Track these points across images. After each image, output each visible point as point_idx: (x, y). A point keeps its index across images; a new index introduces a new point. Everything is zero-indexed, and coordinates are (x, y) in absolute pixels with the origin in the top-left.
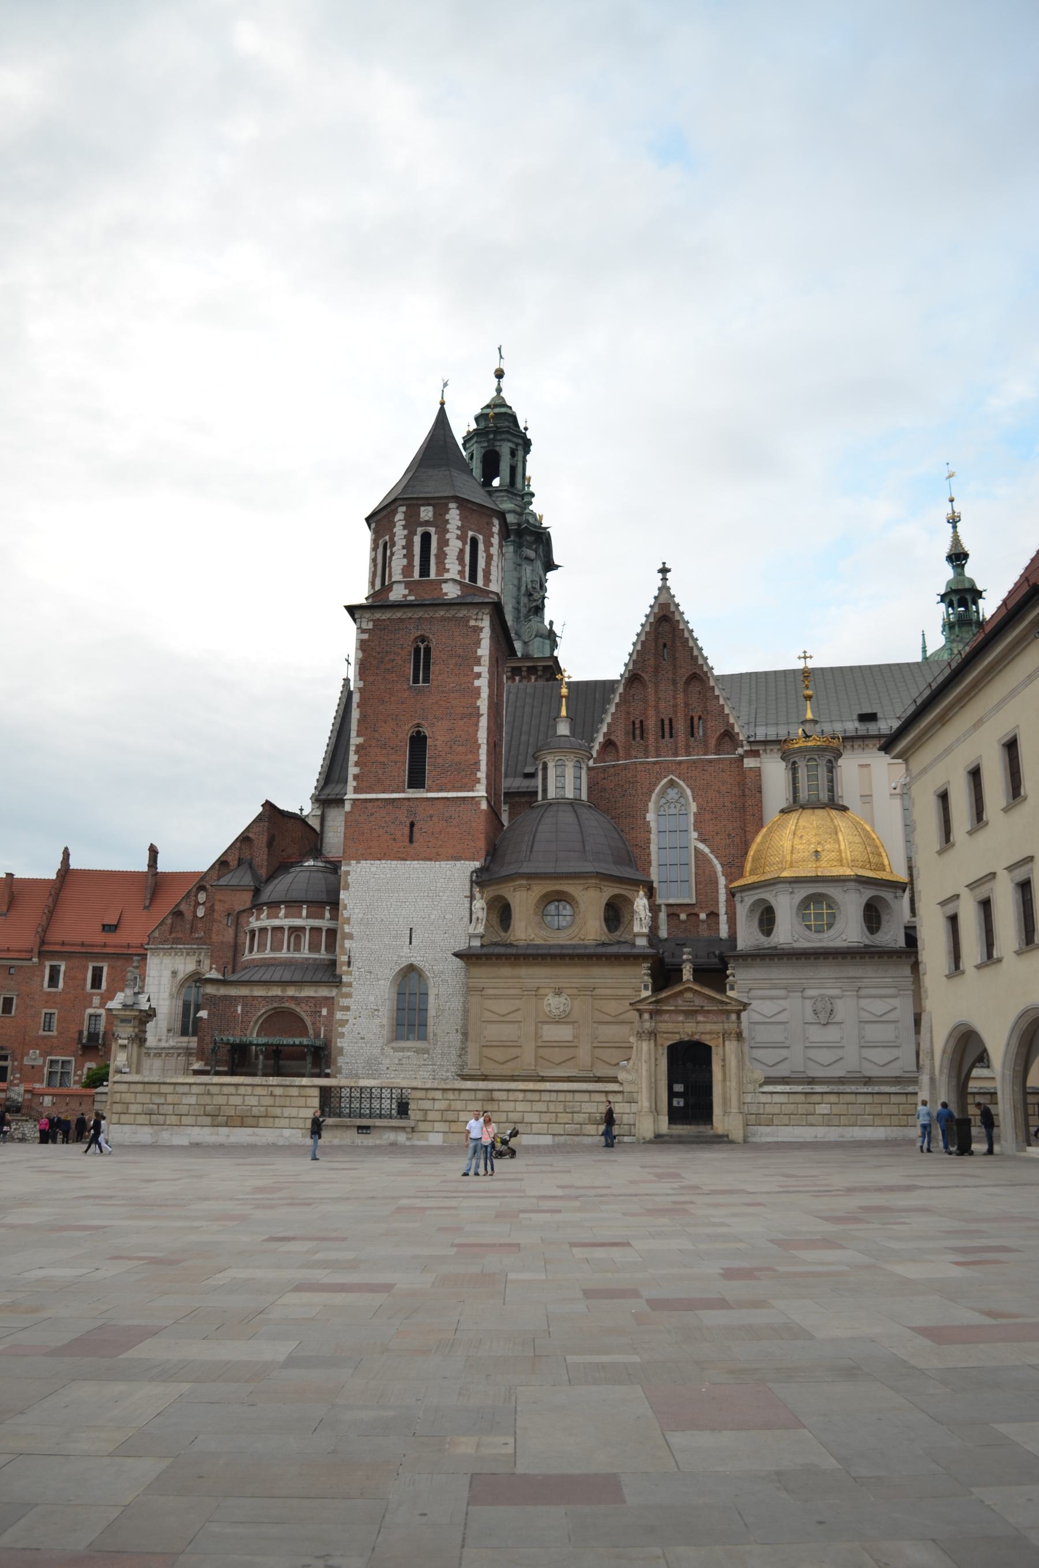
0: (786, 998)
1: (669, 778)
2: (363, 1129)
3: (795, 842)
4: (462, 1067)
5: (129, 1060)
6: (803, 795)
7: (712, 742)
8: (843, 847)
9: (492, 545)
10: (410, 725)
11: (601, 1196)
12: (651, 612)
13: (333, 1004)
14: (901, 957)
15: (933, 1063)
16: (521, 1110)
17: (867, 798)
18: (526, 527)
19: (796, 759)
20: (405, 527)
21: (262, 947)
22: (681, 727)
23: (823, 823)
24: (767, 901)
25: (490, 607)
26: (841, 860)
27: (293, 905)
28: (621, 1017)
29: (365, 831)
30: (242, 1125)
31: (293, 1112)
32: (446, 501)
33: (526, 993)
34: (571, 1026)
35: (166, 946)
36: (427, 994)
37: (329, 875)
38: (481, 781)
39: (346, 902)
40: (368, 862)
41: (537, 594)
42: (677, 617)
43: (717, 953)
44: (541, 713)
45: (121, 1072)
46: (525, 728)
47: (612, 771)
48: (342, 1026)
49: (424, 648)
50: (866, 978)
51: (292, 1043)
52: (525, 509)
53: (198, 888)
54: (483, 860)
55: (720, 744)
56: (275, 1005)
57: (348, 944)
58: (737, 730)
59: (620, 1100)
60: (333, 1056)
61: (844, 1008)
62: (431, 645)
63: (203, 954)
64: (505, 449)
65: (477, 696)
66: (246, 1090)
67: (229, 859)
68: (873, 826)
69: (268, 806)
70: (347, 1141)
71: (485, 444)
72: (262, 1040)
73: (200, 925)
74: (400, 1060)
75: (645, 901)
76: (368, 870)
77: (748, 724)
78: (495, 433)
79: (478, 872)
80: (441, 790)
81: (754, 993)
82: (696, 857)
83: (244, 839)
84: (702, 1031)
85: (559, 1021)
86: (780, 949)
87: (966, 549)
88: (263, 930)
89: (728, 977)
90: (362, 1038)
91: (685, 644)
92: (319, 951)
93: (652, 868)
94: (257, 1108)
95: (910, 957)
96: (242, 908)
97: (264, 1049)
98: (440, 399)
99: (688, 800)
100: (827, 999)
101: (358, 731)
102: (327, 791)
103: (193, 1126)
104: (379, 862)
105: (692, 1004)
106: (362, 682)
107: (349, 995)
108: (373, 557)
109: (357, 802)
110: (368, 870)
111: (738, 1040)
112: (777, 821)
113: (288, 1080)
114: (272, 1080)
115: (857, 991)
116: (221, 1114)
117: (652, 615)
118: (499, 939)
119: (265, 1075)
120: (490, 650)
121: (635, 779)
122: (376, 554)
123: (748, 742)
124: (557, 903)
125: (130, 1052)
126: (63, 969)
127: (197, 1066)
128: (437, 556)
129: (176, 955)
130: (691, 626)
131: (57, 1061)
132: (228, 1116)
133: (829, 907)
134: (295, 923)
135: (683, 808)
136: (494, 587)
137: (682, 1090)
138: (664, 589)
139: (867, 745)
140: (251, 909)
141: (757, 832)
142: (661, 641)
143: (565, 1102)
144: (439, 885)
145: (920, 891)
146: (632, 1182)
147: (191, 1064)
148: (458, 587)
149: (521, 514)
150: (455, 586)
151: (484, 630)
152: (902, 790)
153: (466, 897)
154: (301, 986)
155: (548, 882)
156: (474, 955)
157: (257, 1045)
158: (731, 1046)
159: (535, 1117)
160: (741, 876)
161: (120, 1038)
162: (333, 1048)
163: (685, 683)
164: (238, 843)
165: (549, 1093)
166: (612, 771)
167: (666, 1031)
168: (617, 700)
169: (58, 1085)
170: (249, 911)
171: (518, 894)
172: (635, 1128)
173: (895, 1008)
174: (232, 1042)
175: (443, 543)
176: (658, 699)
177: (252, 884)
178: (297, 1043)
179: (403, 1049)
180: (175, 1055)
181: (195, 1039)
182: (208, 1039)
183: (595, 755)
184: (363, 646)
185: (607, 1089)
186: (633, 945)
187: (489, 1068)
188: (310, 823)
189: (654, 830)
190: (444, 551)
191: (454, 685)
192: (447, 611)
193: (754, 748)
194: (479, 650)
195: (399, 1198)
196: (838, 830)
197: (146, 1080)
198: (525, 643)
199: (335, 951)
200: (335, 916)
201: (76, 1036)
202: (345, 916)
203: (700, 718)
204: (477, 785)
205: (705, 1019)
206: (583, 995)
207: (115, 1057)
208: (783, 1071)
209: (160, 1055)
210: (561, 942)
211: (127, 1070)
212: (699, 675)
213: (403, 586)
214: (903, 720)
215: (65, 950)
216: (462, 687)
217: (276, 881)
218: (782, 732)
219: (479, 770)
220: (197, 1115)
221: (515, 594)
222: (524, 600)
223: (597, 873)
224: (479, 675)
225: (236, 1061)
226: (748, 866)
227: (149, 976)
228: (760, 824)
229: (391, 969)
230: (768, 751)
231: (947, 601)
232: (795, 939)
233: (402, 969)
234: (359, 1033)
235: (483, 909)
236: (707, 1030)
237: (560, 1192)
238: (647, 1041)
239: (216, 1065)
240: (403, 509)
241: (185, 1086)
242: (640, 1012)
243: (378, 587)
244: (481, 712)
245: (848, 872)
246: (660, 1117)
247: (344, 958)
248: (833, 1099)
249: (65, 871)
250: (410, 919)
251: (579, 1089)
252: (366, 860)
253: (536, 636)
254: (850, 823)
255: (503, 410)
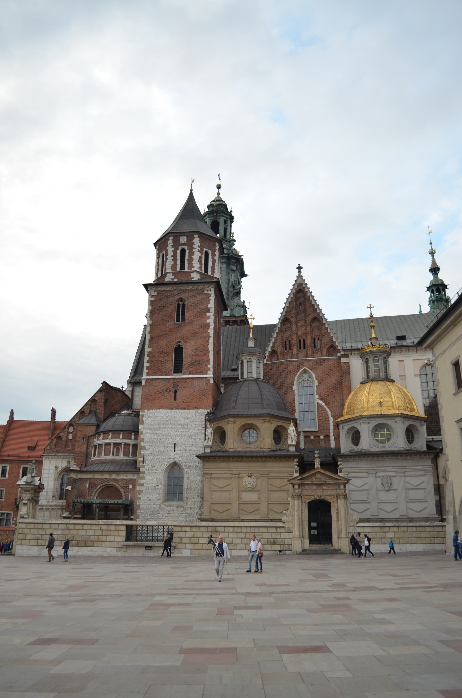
0: (367, 477)
1: (304, 368)
2: (148, 548)
3: (369, 398)
4: (201, 514)
5: (28, 511)
6: (372, 375)
7: (325, 350)
8: (394, 400)
9: (215, 255)
10: (175, 342)
11: (286, 592)
12: (293, 288)
13: (135, 482)
14: (426, 455)
15: (455, 509)
16: (231, 537)
17: (403, 377)
18: (232, 255)
19: (368, 357)
20: (173, 246)
21: (100, 454)
22: (309, 343)
23: (383, 388)
24: (356, 427)
25: (215, 284)
26: (393, 406)
27: (116, 432)
28: (282, 488)
29: (152, 395)
30: (85, 546)
31: (112, 539)
32: (193, 234)
33: (233, 476)
34: (257, 493)
35: (52, 454)
36: (183, 477)
37: (134, 418)
38: (210, 370)
39: (142, 430)
40: (153, 410)
41: (236, 286)
42: (306, 290)
43: (331, 454)
44: (240, 340)
45: (23, 518)
46: (232, 347)
47: (275, 365)
48: (140, 494)
49: (182, 305)
50: (408, 466)
51: (113, 502)
52: (231, 247)
53: (69, 425)
54: (211, 409)
55: (328, 352)
56: (106, 483)
57: (143, 452)
58: (337, 344)
59: (284, 531)
60: (135, 510)
61: (398, 482)
62: (185, 303)
63: (71, 458)
64: (221, 220)
65: (208, 327)
66: (87, 527)
67: (85, 410)
68: (406, 389)
69: (105, 384)
70: (140, 554)
71: (212, 218)
72: (98, 501)
73: (70, 444)
74: (169, 511)
75: (294, 428)
76: (153, 414)
77: (342, 342)
78: (217, 213)
79: (208, 414)
80: (190, 374)
81: (351, 475)
82: (318, 408)
83: (93, 400)
84: (326, 494)
85: (251, 490)
86: (363, 452)
87: (439, 266)
88: (100, 445)
89: (338, 466)
90: (150, 500)
91: (310, 303)
92: (129, 455)
93: (296, 414)
94: (93, 536)
95: (431, 455)
96: (90, 434)
97: (99, 506)
98: (190, 188)
99: (314, 379)
100: (388, 477)
101: (149, 345)
102: (135, 378)
103: (59, 546)
104: (159, 410)
105: (320, 480)
106: (151, 321)
107: (143, 478)
108: (157, 261)
109: (148, 381)
110: (153, 414)
111: (345, 499)
112: (359, 388)
113: (109, 522)
114: (101, 522)
115: (404, 473)
116: (74, 540)
117: (294, 290)
118: (220, 448)
119: (99, 519)
120: (215, 305)
121: (286, 369)
122: (159, 260)
123: (343, 350)
124: (249, 430)
125: (28, 508)
126: (8, 468)
127: (65, 515)
128: (188, 260)
129: (57, 458)
130: (313, 294)
131: (4, 514)
132: (78, 541)
133: (388, 430)
134: (116, 442)
135: (311, 383)
136: (216, 275)
137: (316, 526)
138: (300, 277)
139: (402, 351)
140: (95, 435)
141: (349, 394)
142: (298, 302)
143: (255, 532)
144: (189, 421)
145: (443, 416)
146: (300, 581)
147: (63, 514)
148: (199, 275)
149: (229, 250)
150: (197, 274)
151: (211, 295)
152: (420, 373)
153: (203, 427)
154: (119, 473)
155: (244, 419)
156: (207, 456)
157: (96, 504)
158: (341, 502)
159: (239, 541)
160: (342, 416)
161: (24, 500)
162: (135, 505)
163: (311, 322)
164: (90, 403)
165: (246, 528)
166: (275, 365)
167: (307, 494)
168: (277, 331)
169: (5, 525)
170: (94, 436)
171: (229, 425)
172: (292, 546)
173: (424, 482)
174: (82, 502)
175: (191, 253)
176: (297, 330)
177: (96, 422)
178: (116, 502)
179: (170, 506)
180: (56, 509)
181: (65, 501)
182: (71, 501)
183: (267, 358)
184: (151, 303)
185: (276, 526)
186: (288, 451)
187: (215, 515)
188: (126, 394)
189: (296, 395)
190: (192, 258)
191: (197, 322)
192: (193, 286)
193: (345, 353)
194: (209, 305)
195: (154, 595)
196: (391, 391)
197: (36, 521)
198: (232, 310)
199: (137, 456)
200: (136, 439)
201: (14, 501)
202: (142, 437)
203: (318, 339)
204: (208, 371)
205: (327, 488)
206: (263, 477)
207: (21, 509)
208: (366, 515)
209: (48, 509)
210: (251, 450)
211: (26, 516)
212: (318, 318)
213: (172, 274)
214: (430, 328)
215: (9, 459)
216: (201, 323)
217: (108, 421)
218: (360, 345)
219: (209, 364)
220: (62, 540)
221: (227, 287)
222: (231, 289)
223: (269, 414)
224: (209, 317)
225: (85, 512)
226: (345, 411)
227: (44, 469)
228: (350, 391)
229: (165, 464)
230: (353, 354)
231: (431, 290)
232: (371, 447)
233: (170, 465)
234: (148, 498)
235: (211, 433)
236: (328, 494)
237: (258, 590)
238: (297, 500)
239: (75, 514)
240: (172, 238)
241: (56, 525)
242: (293, 485)
243: (159, 275)
244: (210, 335)
245: (397, 412)
246: (304, 540)
247: (141, 459)
248: (395, 529)
249: (11, 421)
250: (175, 439)
251: (262, 526)
252: (152, 409)
253: (237, 306)
254: (396, 388)
255: (220, 202)
